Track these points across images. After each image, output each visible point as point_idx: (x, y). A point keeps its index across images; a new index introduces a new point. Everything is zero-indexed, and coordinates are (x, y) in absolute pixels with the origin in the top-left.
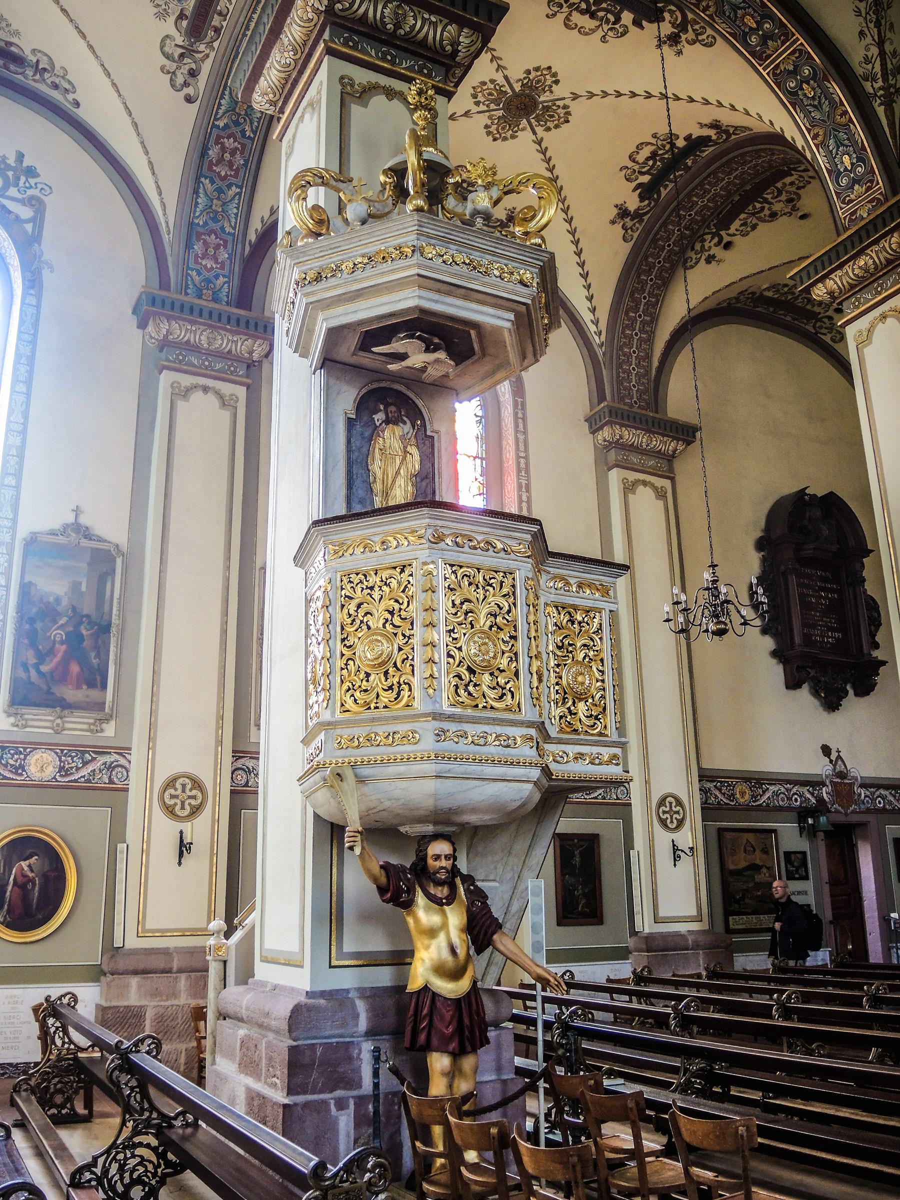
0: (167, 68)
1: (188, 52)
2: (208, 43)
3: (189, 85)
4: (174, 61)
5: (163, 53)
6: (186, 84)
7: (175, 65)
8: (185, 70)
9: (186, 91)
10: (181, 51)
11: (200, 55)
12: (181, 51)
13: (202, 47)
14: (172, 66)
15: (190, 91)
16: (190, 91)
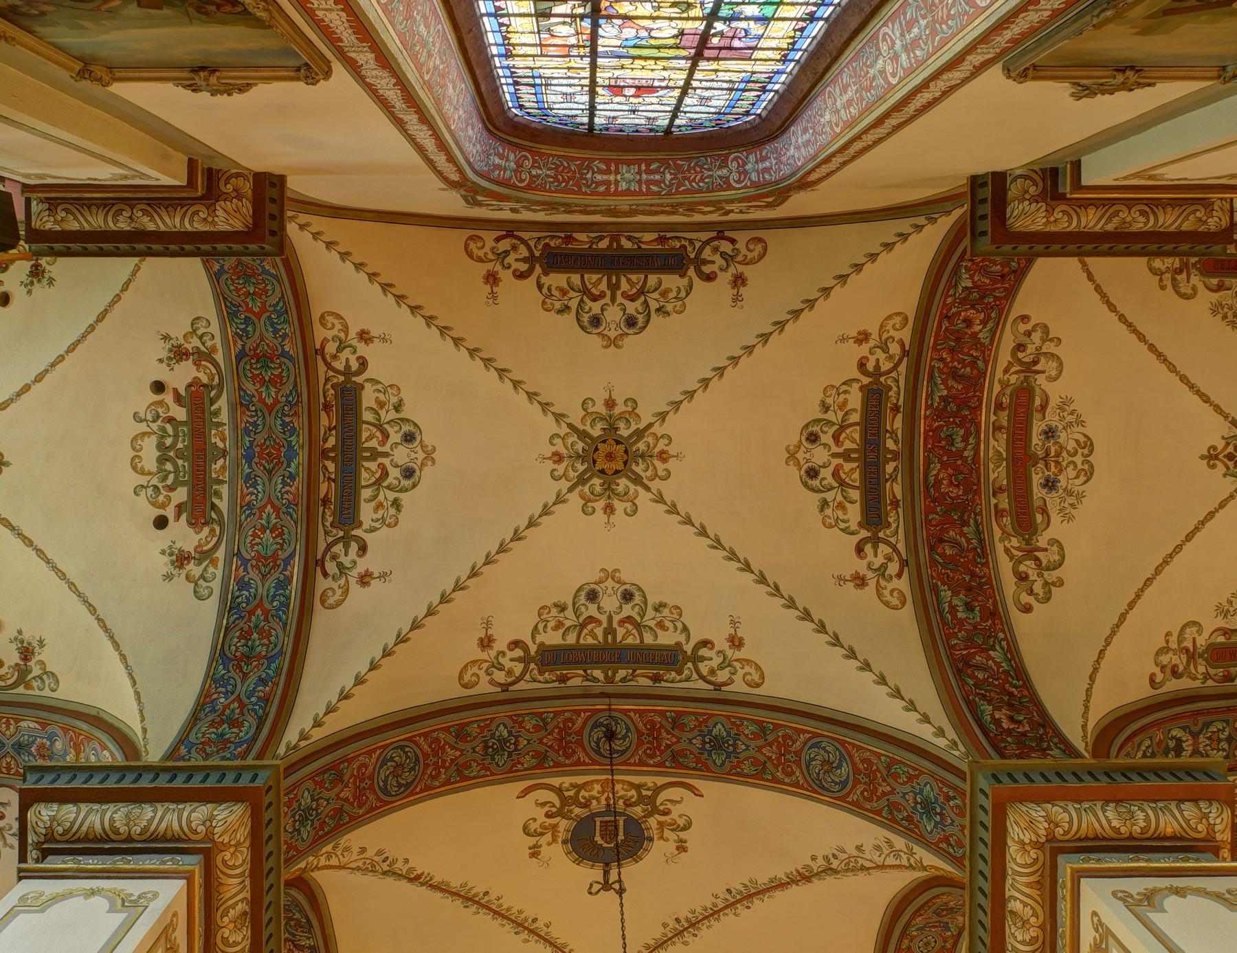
0: (1053, 344)
1: (1029, 368)
2: (1008, 386)
3: (1024, 334)
4: (1045, 354)
5: (1058, 358)
6: (1028, 334)
7: (1044, 350)
8: (1031, 349)
9: (1029, 327)
10: (1038, 367)
11: (1013, 370)
12: (1038, 367)
13: (1013, 379)
14: (1049, 347)
15: (1022, 328)
16: (1022, 328)
